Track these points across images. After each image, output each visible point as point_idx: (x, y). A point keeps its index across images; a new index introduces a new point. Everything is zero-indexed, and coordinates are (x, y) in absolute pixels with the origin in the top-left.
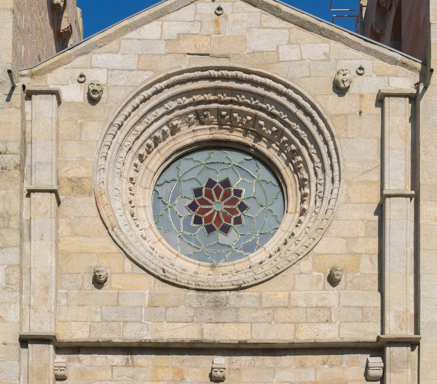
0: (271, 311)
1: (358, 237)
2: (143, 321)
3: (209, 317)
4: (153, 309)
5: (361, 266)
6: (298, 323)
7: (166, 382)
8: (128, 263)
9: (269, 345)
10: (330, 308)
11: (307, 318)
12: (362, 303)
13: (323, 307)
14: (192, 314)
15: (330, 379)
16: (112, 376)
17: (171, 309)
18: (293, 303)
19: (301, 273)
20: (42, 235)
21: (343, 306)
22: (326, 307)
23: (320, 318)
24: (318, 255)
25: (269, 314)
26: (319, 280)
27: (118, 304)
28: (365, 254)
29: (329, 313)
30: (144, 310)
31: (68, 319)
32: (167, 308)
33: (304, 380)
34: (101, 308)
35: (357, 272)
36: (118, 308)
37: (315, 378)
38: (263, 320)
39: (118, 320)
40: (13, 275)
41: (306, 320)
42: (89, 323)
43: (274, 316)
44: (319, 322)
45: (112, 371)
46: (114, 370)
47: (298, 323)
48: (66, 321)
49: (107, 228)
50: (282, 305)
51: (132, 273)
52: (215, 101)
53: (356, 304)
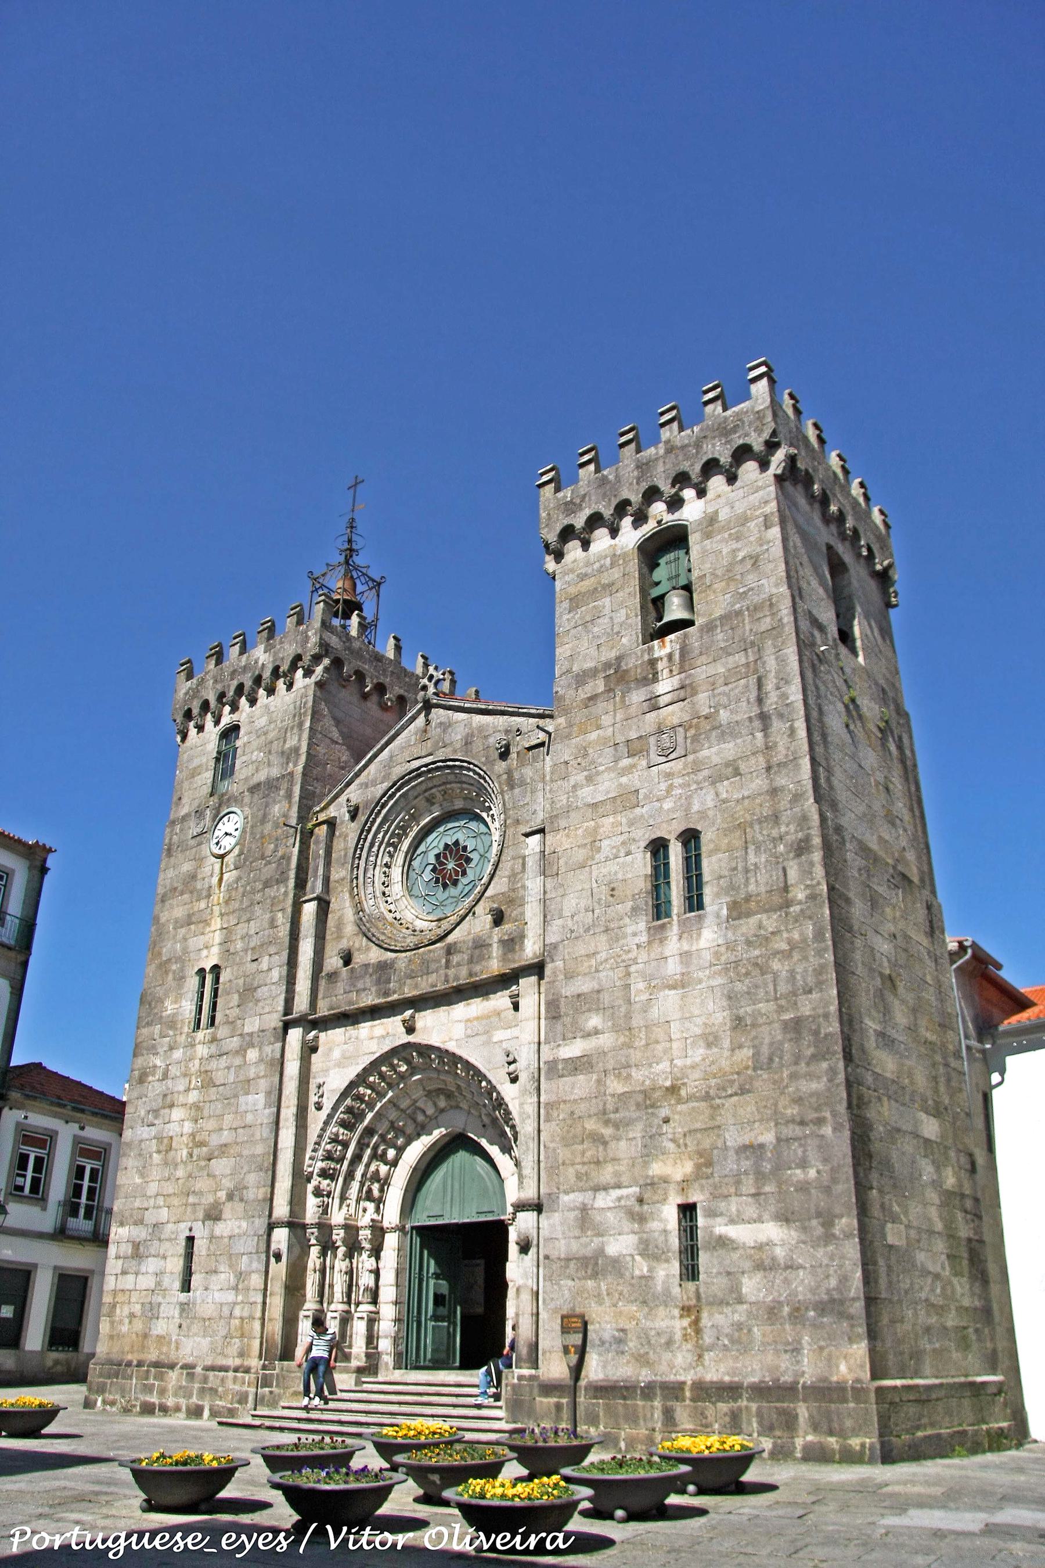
52: (435, 786)
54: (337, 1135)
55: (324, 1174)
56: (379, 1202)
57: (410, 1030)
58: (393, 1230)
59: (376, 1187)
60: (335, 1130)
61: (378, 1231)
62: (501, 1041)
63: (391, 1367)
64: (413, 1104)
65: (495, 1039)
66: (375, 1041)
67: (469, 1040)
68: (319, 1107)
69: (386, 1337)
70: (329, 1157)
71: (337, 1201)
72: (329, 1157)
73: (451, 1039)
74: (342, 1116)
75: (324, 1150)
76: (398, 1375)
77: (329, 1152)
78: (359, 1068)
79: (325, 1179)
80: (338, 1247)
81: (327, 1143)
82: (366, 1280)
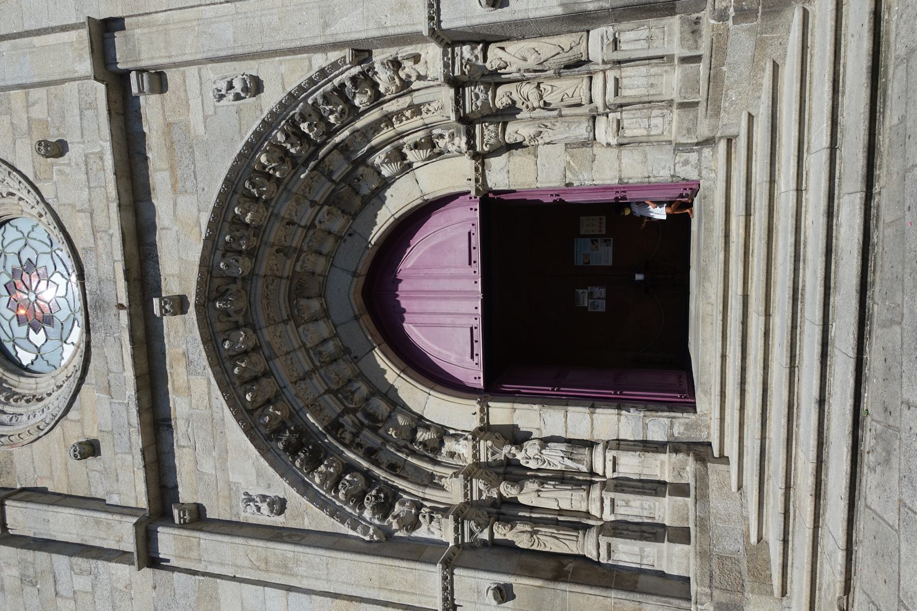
0: (98, 235)
1: (12, 124)
2: (126, 401)
3: (113, 317)
4: (112, 389)
5: (41, 117)
6: (107, 198)
7: (190, 377)
8: (72, 414)
9: (127, 238)
10: (86, 156)
11: (101, 187)
12: (77, 112)
13: (86, 165)
14: (112, 339)
15: (165, 149)
16: (189, 447)
17: (110, 367)
18: (86, 206)
19: (56, 197)
20: (44, 520)
21: (82, 137)
22: (86, 161)
23: (99, 168)
24: (36, 176)
25: (101, 238)
26: (61, 172)
27: (111, 432)
28: (28, 113)
29: (92, 156)
30: (114, 401)
31: (133, 495)
32: (109, 371)
33: (170, 186)
34: (116, 454)
35: (47, 121)
36: (115, 432)
37: (166, 170)
38: (109, 246)
39: (128, 433)
40: (80, 565)
41: (103, 187)
42: (135, 469)
43: (103, 231)
44: (104, 170)
45: (184, 447)
46: (182, 444)
47: (107, 198)
48: (137, 497)
49: (39, 438)
50: (90, 221)
51: (81, 409)
53: (78, 118)
54: (325, 477)
55: (384, 508)
56: (443, 432)
57: (180, 305)
58: (485, 412)
59: (422, 435)
60: (317, 480)
61: (486, 430)
62: (205, 118)
63: (692, 417)
64: (307, 350)
65: (201, 130)
66: (192, 378)
67: (201, 185)
68: (279, 506)
69: (645, 427)
70: (358, 500)
71: (431, 494)
72: (358, 500)
73: (198, 223)
74: (297, 464)
75: (346, 503)
76: (707, 401)
77: (349, 497)
78: (228, 413)
79: (392, 507)
80: (500, 494)
81: (337, 497)
82: (555, 458)
